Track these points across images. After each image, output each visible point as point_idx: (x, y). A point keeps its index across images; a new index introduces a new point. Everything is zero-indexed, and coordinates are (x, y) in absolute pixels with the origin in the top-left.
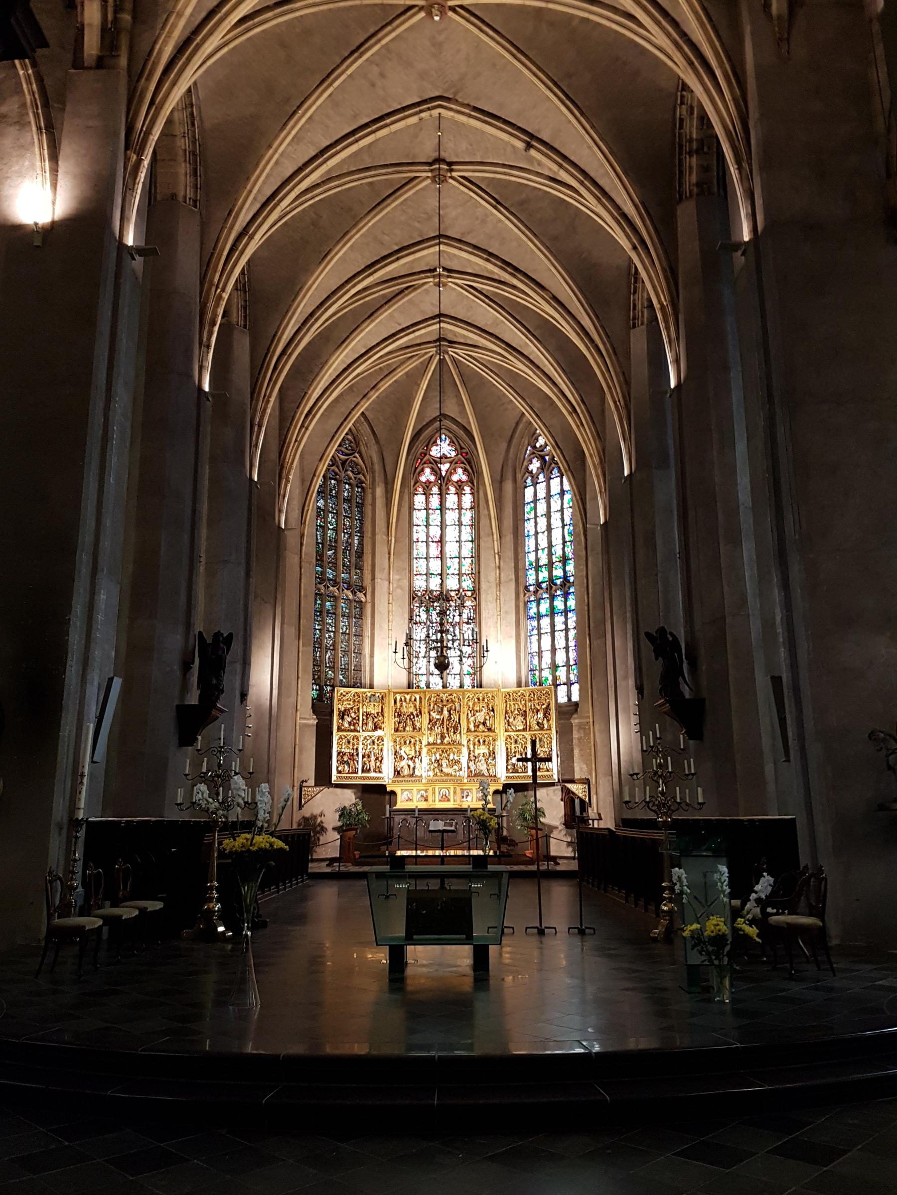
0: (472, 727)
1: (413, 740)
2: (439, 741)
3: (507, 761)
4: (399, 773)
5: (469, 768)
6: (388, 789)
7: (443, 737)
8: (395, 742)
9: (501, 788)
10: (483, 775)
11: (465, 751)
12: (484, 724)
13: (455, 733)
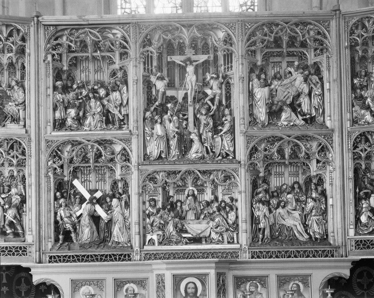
0: (262, 114)
1: (106, 155)
2: (174, 152)
3: (358, 200)
4: (67, 234)
5: (254, 220)
6: (36, 279)
7: (185, 144)
8: (56, 154)
9: (346, 273)
10: (293, 240)
11: (243, 180)
12: (295, 107)
13: (216, 131)
